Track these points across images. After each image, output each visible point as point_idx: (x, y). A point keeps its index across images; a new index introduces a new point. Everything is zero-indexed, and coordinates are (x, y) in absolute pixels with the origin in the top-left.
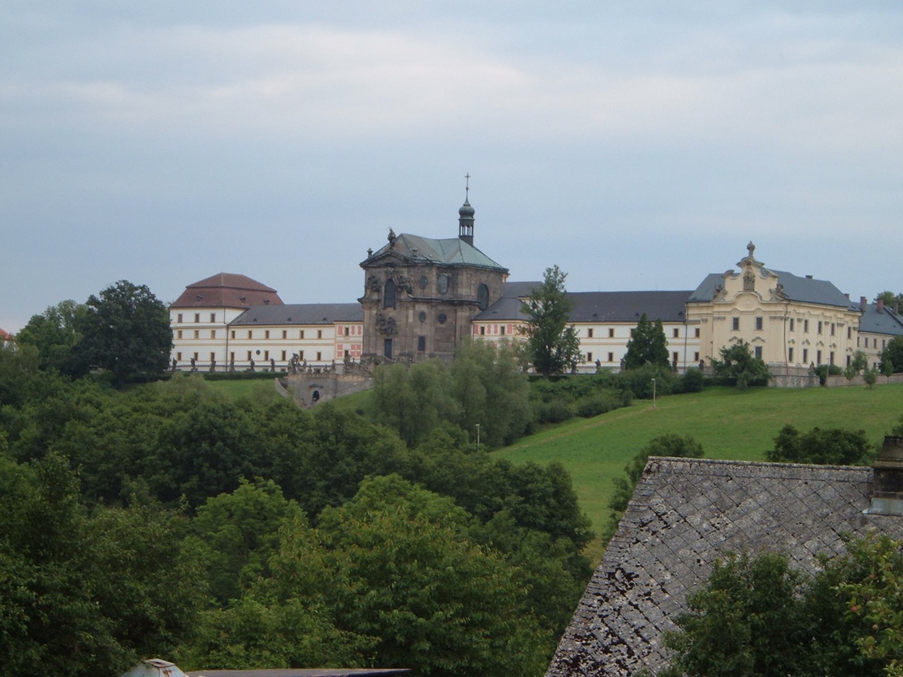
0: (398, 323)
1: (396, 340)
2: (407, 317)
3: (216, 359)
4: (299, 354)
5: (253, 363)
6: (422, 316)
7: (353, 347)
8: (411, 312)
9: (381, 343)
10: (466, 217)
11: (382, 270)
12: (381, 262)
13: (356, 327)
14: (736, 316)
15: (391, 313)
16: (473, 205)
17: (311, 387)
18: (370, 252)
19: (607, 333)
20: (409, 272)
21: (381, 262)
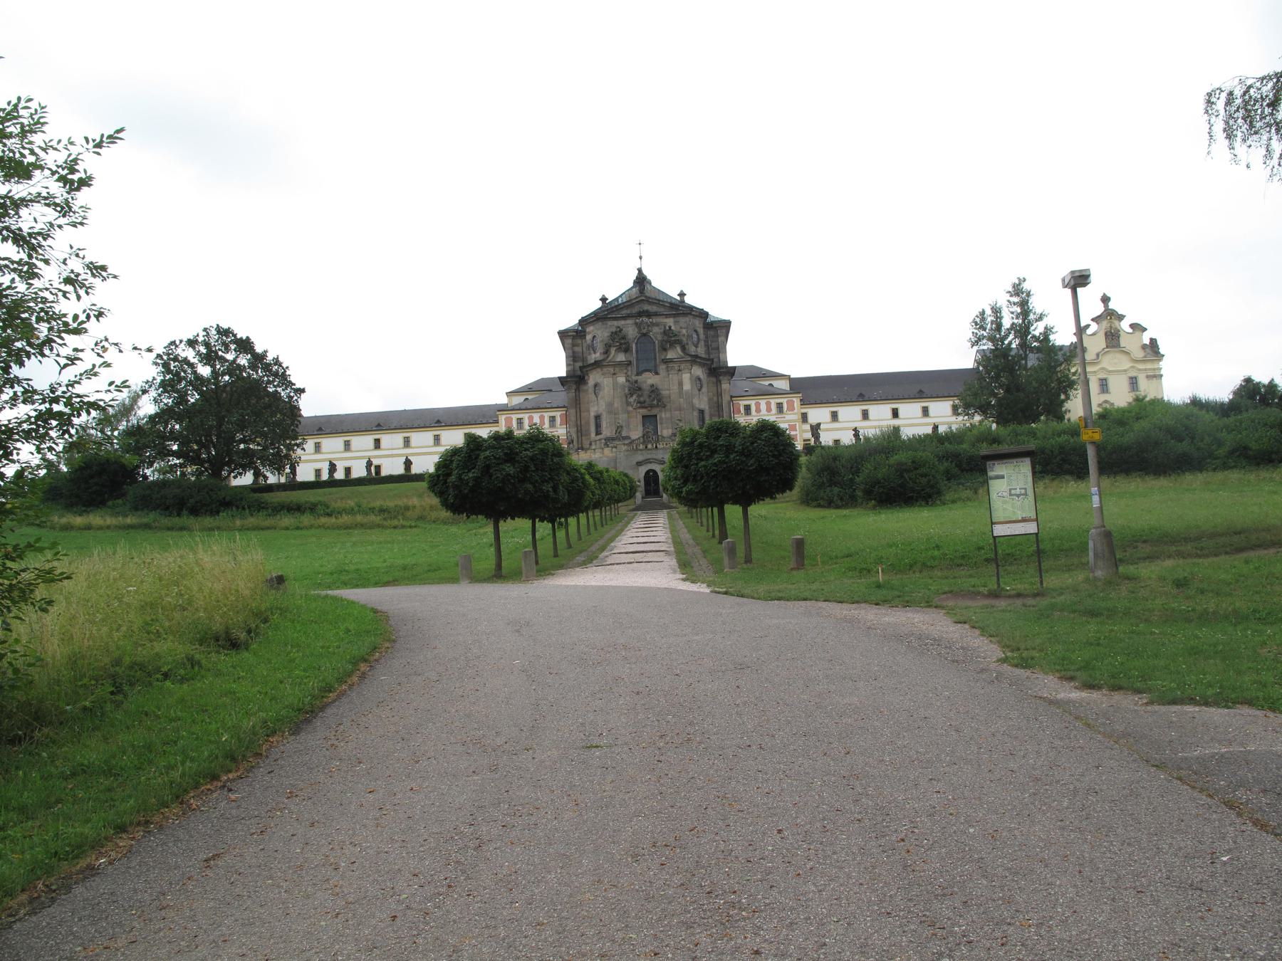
0: (665, 393)
1: (663, 415)
2: (681, 384)
8: (686, 377)
11: (630, 322)
12: (625, 312)
14: (1102, 376)
15: (649, 379)
17: (639, 464)
19: (890, 414)
20: (676, 322)
21: (625, 312)
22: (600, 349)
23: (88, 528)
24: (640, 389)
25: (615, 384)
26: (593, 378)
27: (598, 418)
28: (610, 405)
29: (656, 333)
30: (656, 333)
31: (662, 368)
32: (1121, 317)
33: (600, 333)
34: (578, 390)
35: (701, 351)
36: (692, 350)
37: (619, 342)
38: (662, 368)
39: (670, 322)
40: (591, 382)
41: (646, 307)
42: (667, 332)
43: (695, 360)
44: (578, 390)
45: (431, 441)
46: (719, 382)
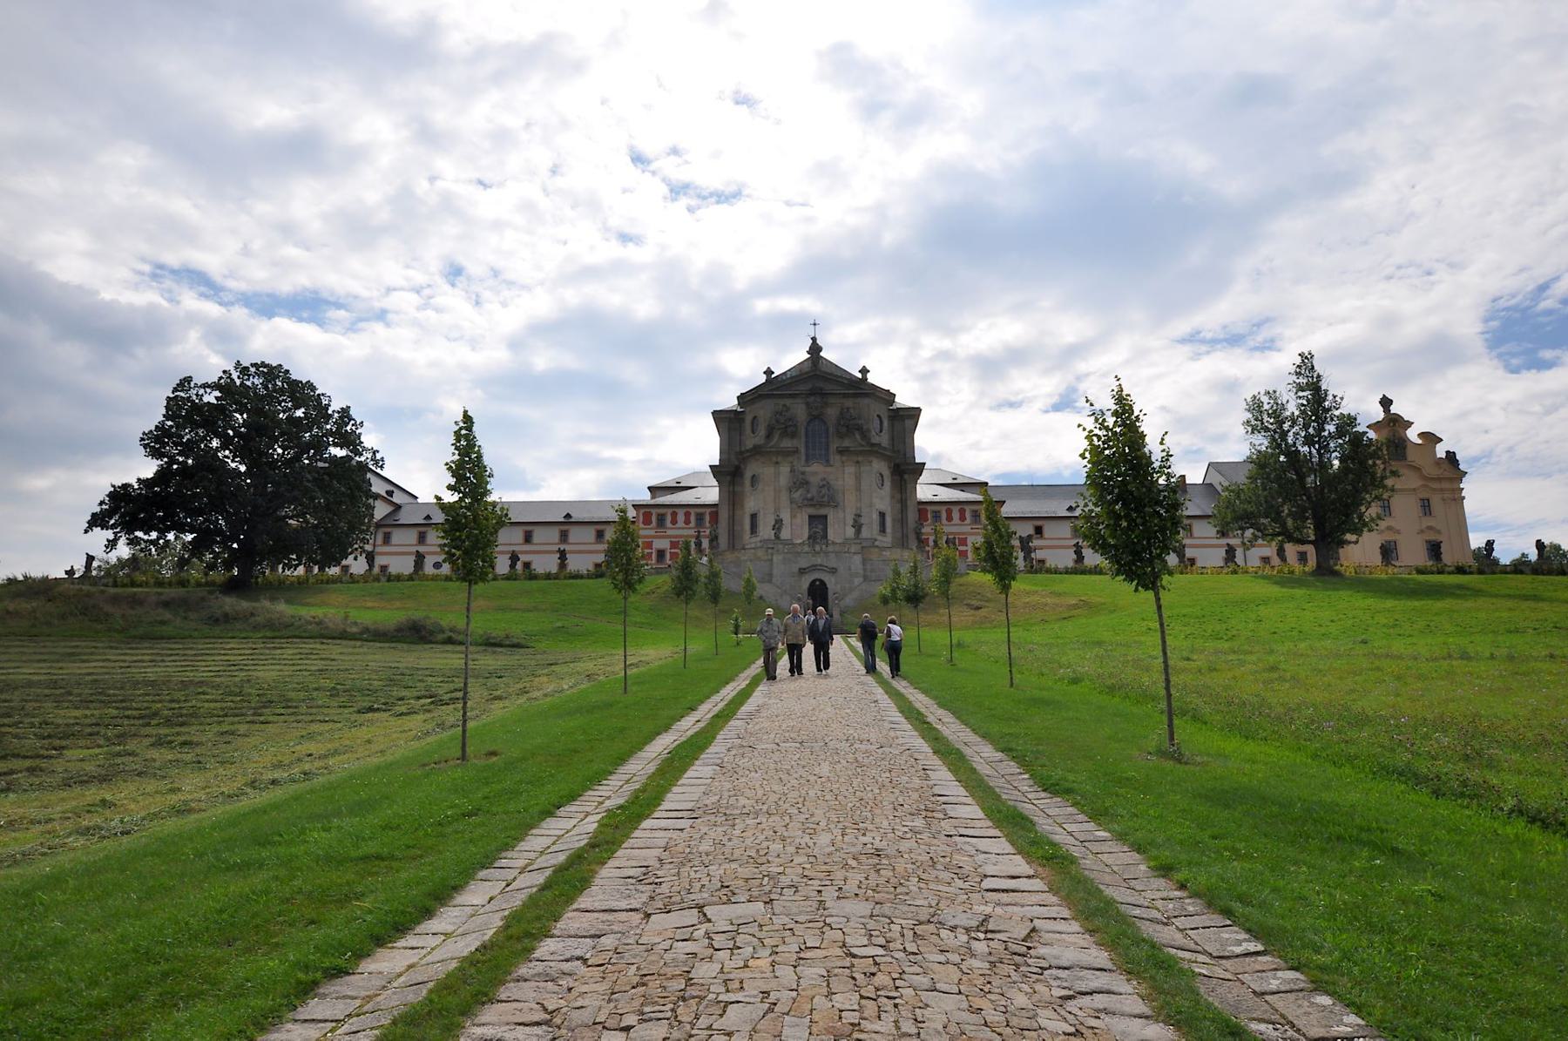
7: (674, 545)
9: (802, 518)
15: (816, 471)
17: (802, 571)
18: (769, 372)
22: (762, 432)
24: (807, 483)
26: (751, 469)
27: (754, 517)
29: (832, 413)
30: (832, 413)
32: (1409, 424)
33: (764, 411)
34: (732, 483)
37: (783, 426)
38: (836, 459)
40: (748, 475)
41: (821, 384)
43: (874, 450)
44: (732, 483)
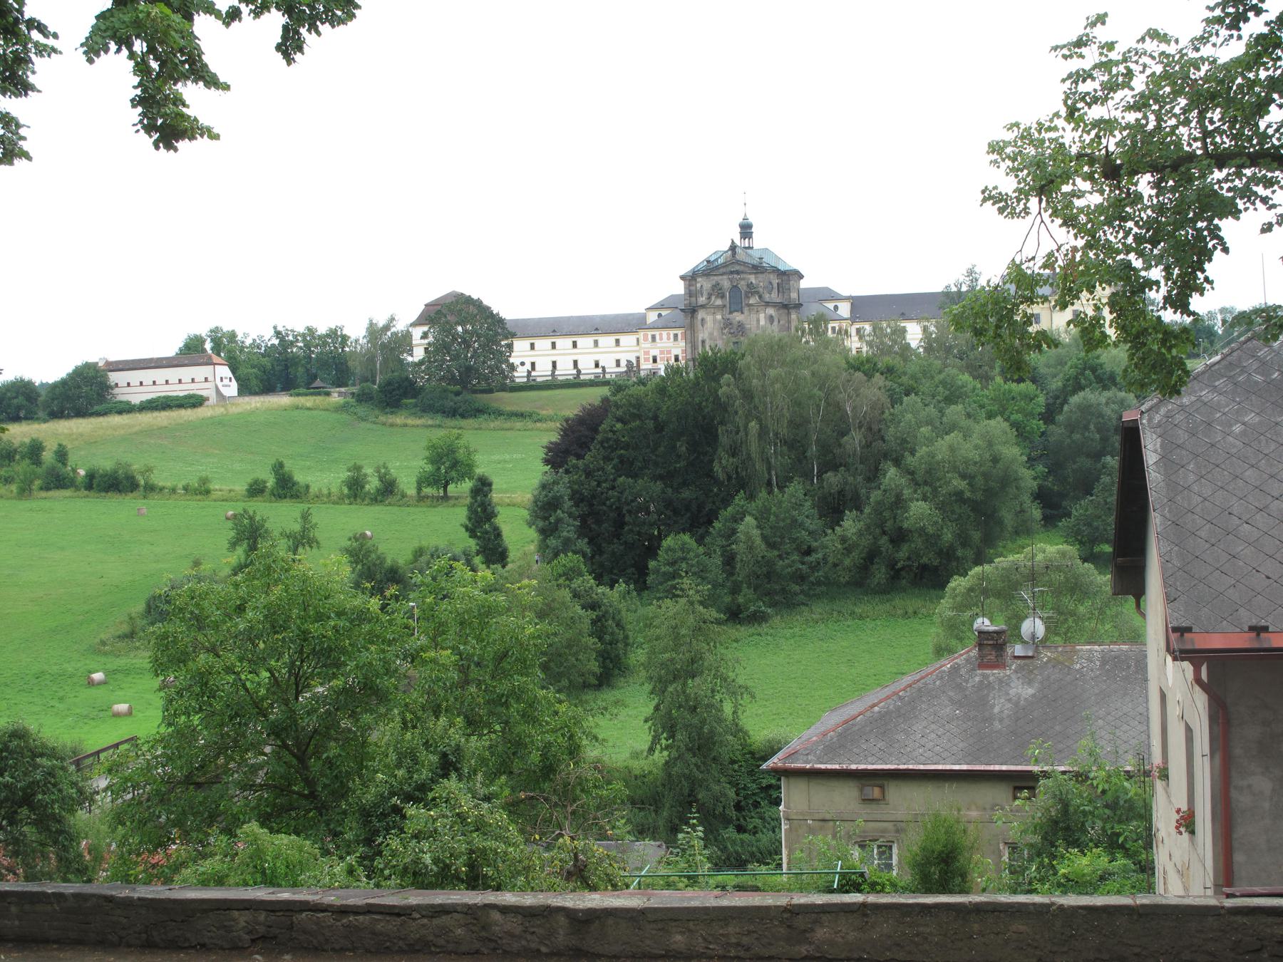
2: (758, 320)
3: (580, 367)
4: (634, 362)
5: (579, 372)
6: (771, 319)
7: (662, 352)
8: (762, 316)
10: (746, 230)
12: (721, 271)
13: (665, 333)
15: (738, 317)
16: (751, 220)
21: (721, 271)
23: (406, 425)
25: (715, 320)
26: (701, 314)
27: (703, 342)
28: (711, 334)
29: (742, 285)
31: (746, 310)
33: (704, 284)
35: (774, 297)
36: (767, 297)
37: (717, 291)
39: (752, 279)
41: (737, 268)
42: (750, 285)
43: (768, 304)
44: (692, 317)
45: (592, 344)
46: (789, 314)
